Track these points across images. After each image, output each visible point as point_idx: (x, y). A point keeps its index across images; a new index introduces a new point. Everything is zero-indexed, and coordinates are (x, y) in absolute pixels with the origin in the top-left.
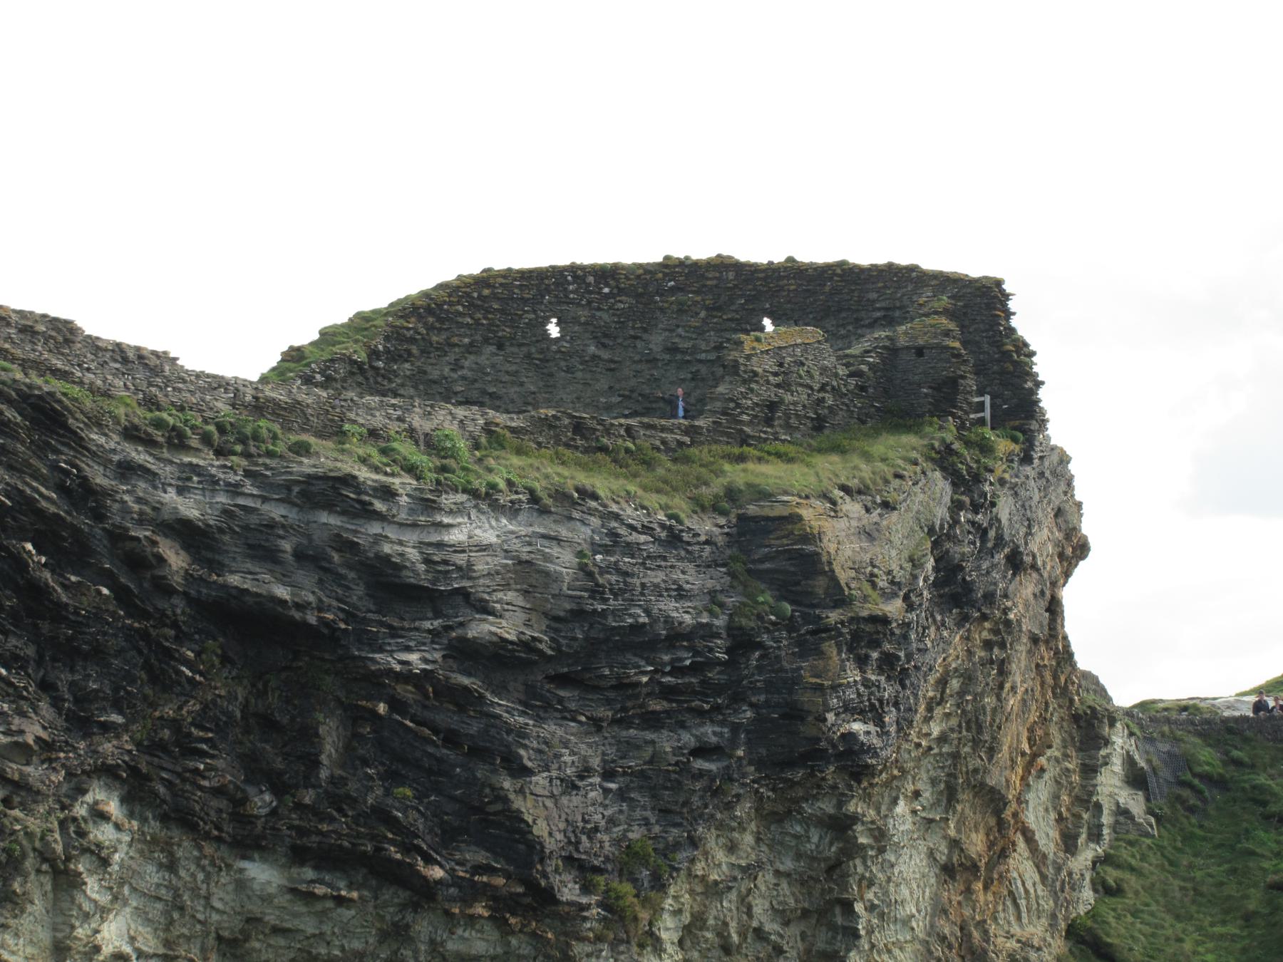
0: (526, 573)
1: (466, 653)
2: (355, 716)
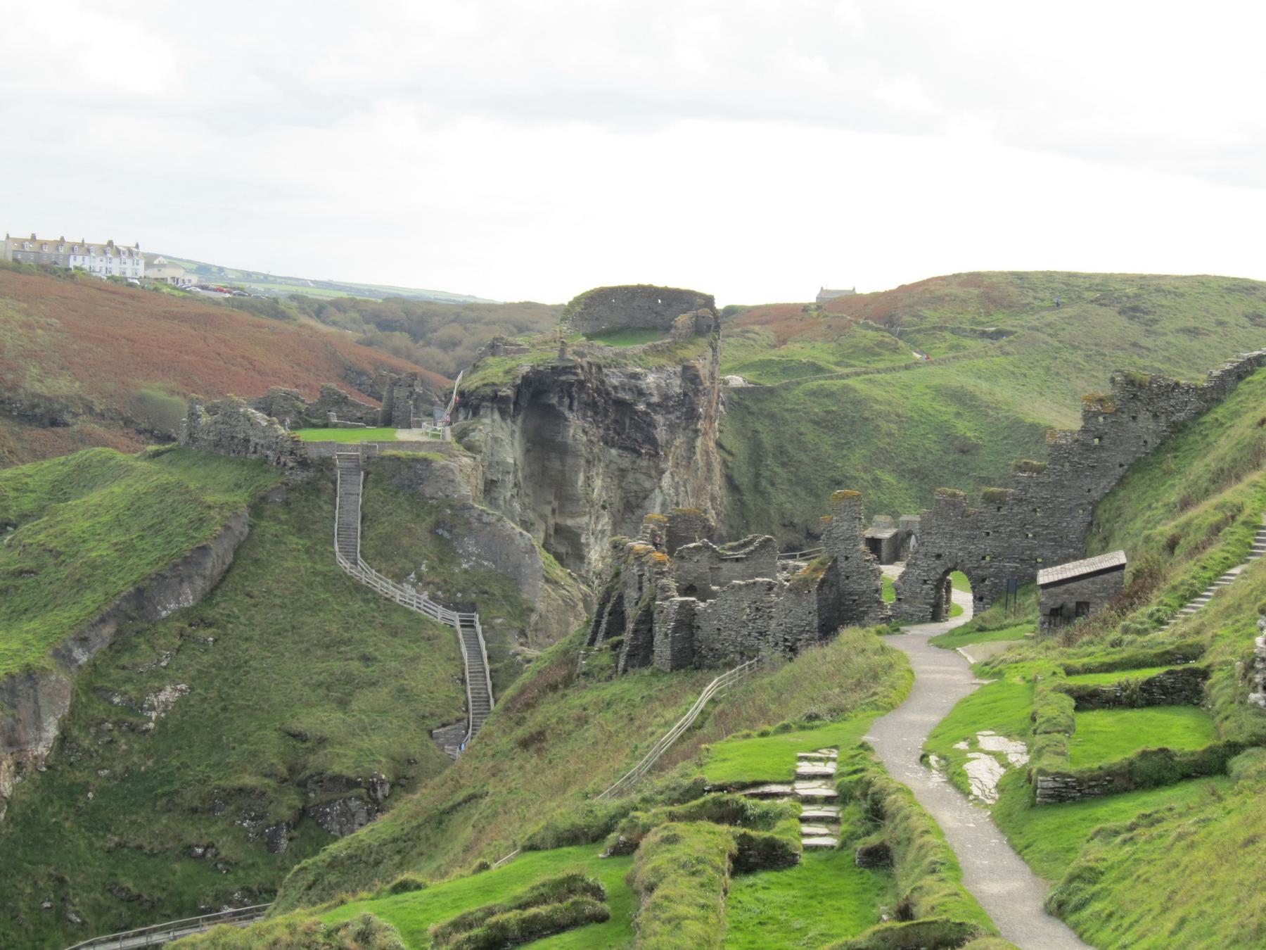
1: (649, 405)
2: (631, 419)
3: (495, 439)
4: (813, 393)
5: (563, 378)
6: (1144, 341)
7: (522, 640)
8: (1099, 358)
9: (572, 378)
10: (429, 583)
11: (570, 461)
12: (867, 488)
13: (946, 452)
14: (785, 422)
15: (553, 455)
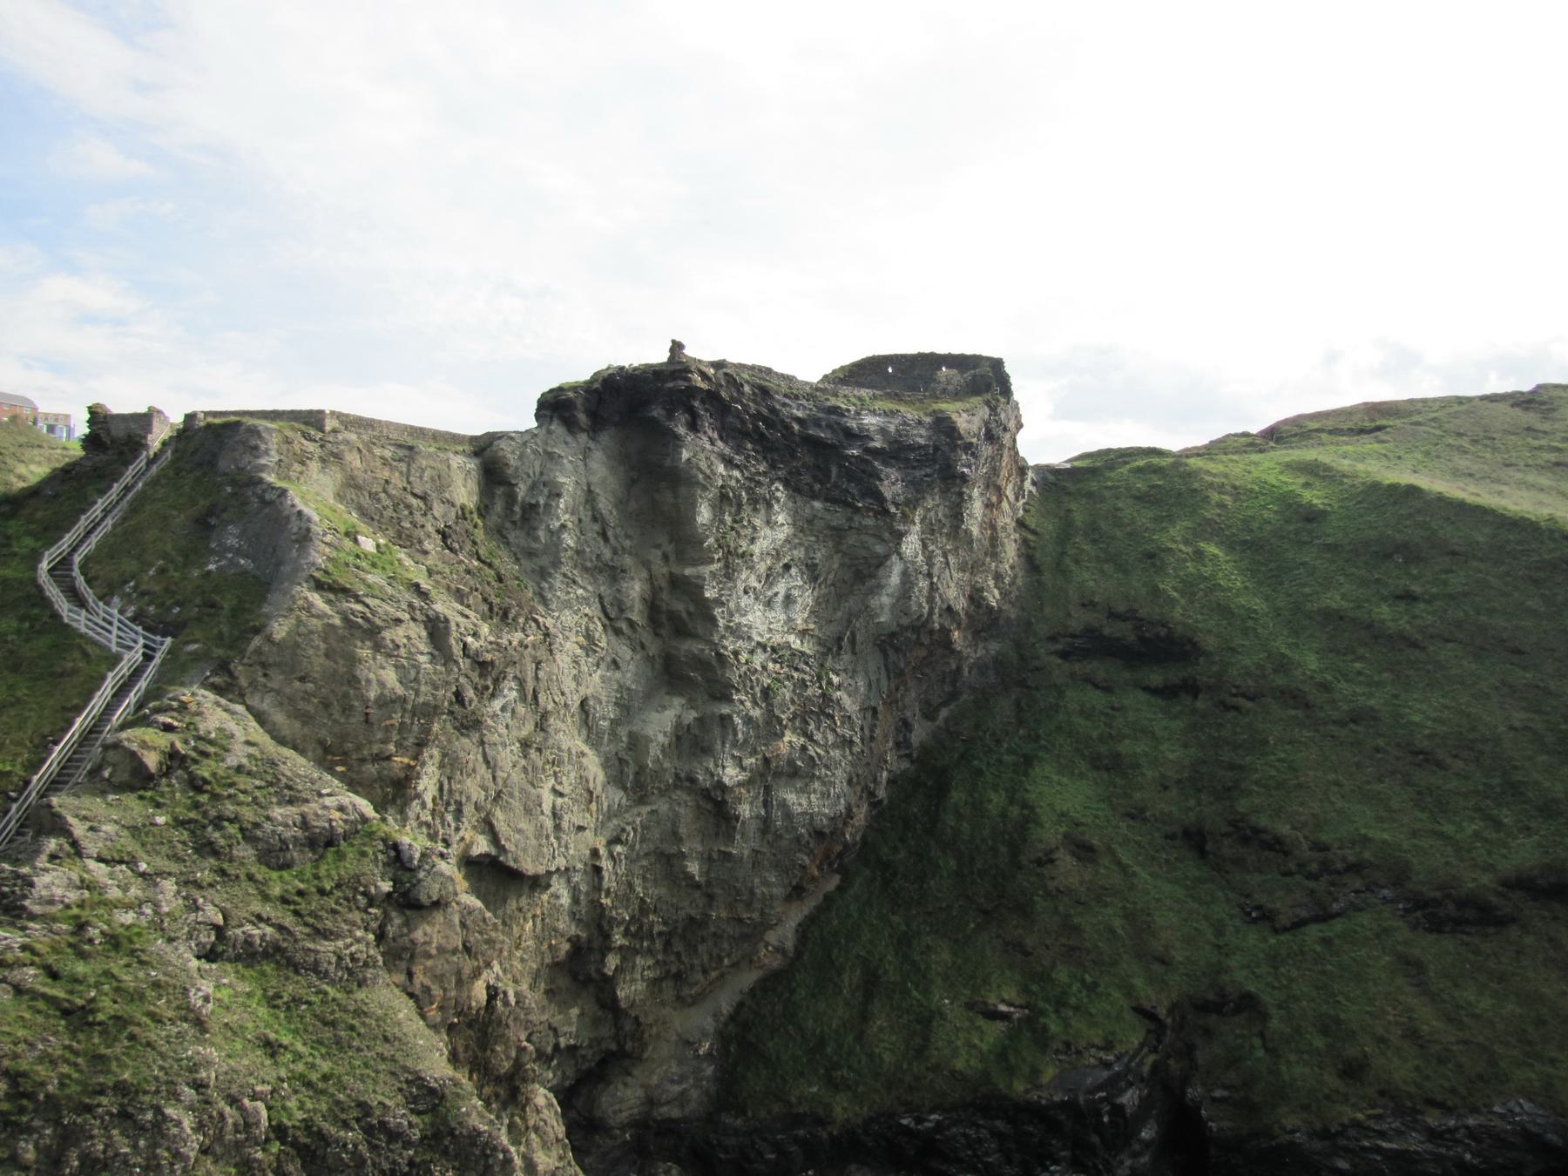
0: (883, 431)
1: (867, 450)
2: (841, 466)
3: (550, 456)
4: (1139, 470)
5: (670, 385)
6: (1538, 426)
7: (217, 680)
8: (1487, 442)
9: (682, 384)
10: (143, 594)
11: (683, 491)
12: (1185, 560)
13: (1288, 521)
14: (1103, 500)
15: (663, 484)
